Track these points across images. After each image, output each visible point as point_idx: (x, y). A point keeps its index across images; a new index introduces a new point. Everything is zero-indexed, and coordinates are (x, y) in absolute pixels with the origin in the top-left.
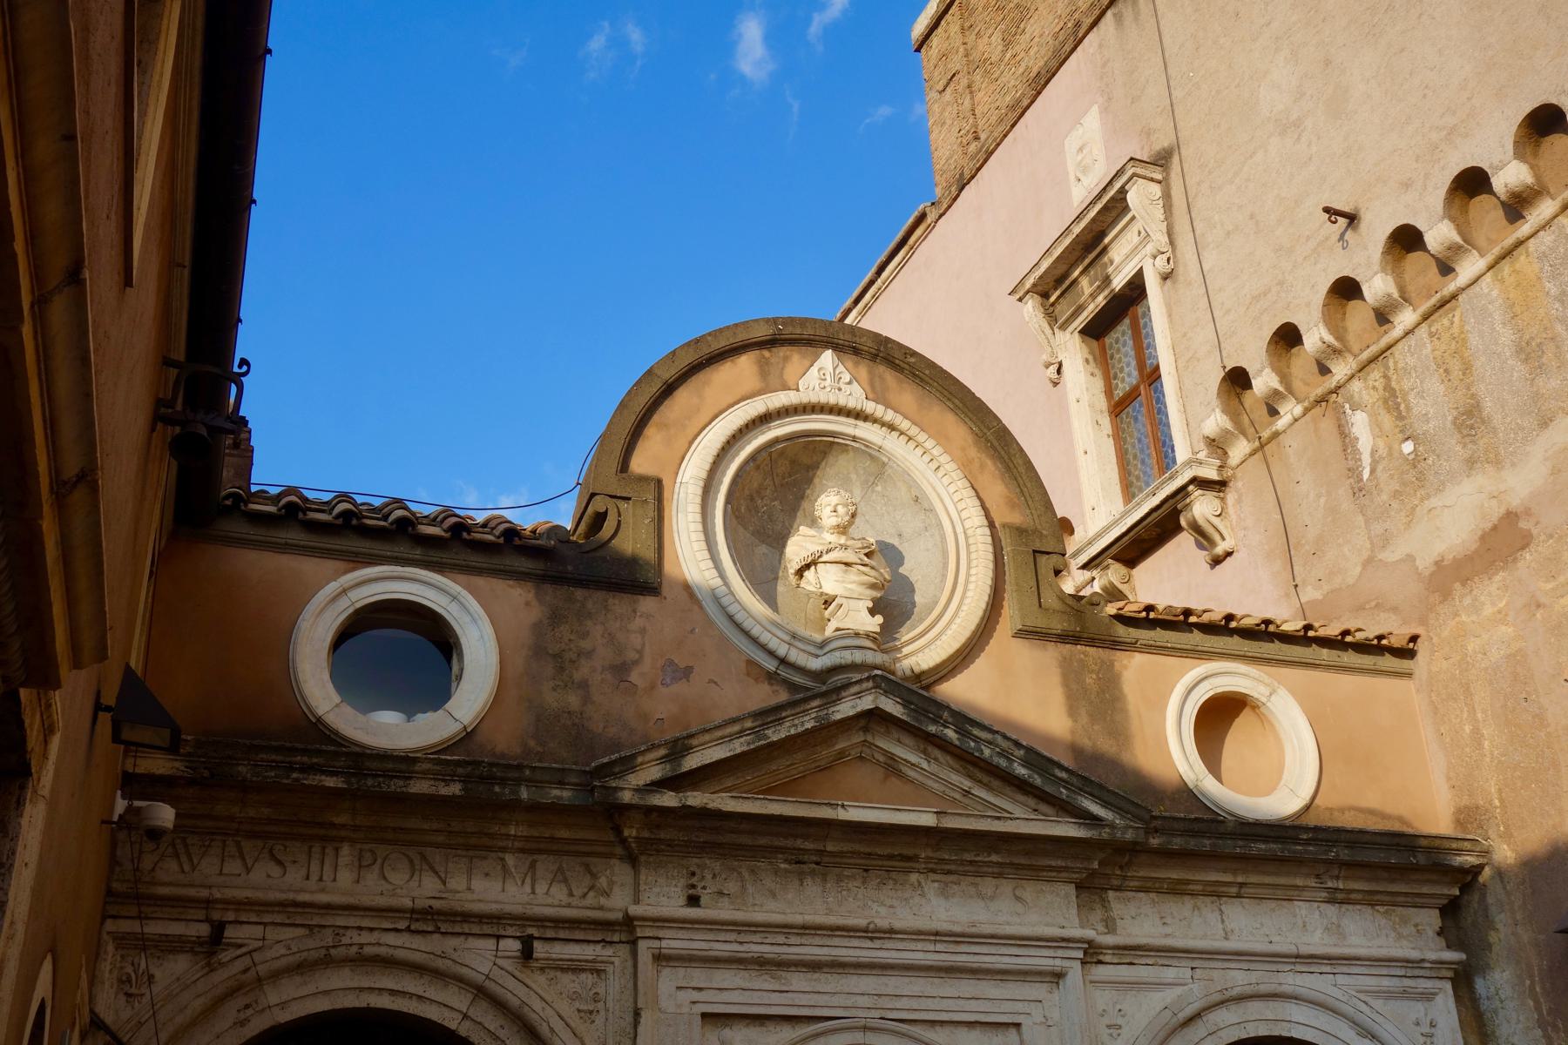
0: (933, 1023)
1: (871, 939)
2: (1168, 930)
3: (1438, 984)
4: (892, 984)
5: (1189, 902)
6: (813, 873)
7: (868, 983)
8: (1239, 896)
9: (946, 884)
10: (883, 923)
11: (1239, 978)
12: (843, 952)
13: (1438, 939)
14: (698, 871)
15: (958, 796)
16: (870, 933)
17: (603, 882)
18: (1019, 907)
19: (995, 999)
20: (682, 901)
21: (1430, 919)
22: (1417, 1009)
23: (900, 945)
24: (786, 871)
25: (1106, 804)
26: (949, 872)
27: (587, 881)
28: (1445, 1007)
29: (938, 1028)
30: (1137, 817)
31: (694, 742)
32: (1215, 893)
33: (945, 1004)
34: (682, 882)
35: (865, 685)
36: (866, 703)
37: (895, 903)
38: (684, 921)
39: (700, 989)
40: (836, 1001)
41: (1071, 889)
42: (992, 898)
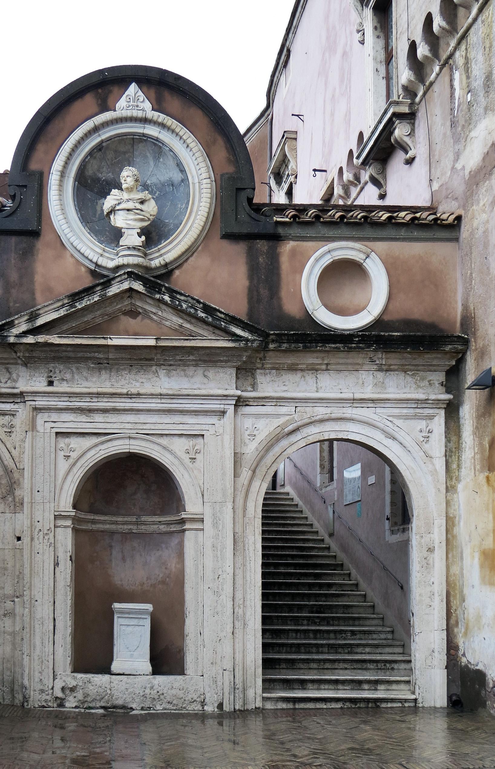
0: (162, 435)
1: (131, 398)
2: (285, 388)
3: (437, 411)
4: (142, 418)
5: (299, 374)
6: (105, 368)
7: (131, 418)
8: (327, 370)
9: (169, 371)
10: (134, 391)
11: (321, 411)
12: (118, 404)
13: (441, 387)
14: (53, 370)
15: (177, 328)
16: (129, 396)
17: (14, 376)
18: (206, 380)
19: (192, 424)
20: (46, 384)
21: (441, 377)
22: (422, 424)
23: (145, 401)
24: (93, 368)
25: (243, 329)
26: (171, 365)
27: (7, 375)
28: (439, 423)
29: (165, 437)
30: (259, 335)
31: (41, 312)
32: (314, 369)
33: (167, 427)
34: (46, 375)
35: (123, 277)
36: (126, 285)
37: (144, 380)
38: (45, 393)
39: (55, 422)
40: (115, 426)
41: (234, 371)
42: (192, 377)
